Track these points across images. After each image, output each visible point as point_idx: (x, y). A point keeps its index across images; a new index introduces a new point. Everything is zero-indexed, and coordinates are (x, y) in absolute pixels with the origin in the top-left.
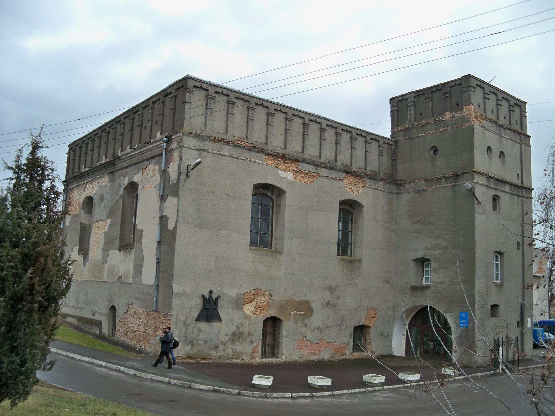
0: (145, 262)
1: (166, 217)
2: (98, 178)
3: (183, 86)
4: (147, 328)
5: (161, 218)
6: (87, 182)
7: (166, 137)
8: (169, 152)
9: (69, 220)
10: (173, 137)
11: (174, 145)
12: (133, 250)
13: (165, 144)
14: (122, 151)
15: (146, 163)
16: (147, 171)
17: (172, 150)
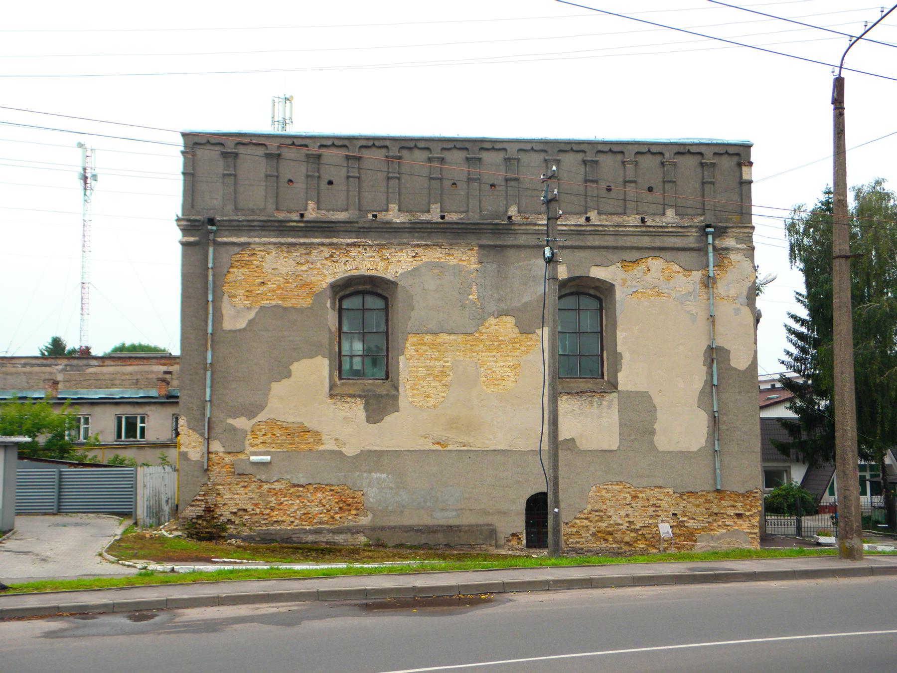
0: (659, 415)
1: (720, 349)
2: (418, 246)
3: (738, 154)
4: (685, 519)
5: (710, 349)
6: (354, 245)
7: (709, 226)
8: (721, 252)
9: (252, 315)
10: (729, 230)
11: (729, 242)
12: (615, 395)
13: (710, 238)
14: (519, 212)
15: (635, 255)
16: (642, 267)
17: (727, 249)
